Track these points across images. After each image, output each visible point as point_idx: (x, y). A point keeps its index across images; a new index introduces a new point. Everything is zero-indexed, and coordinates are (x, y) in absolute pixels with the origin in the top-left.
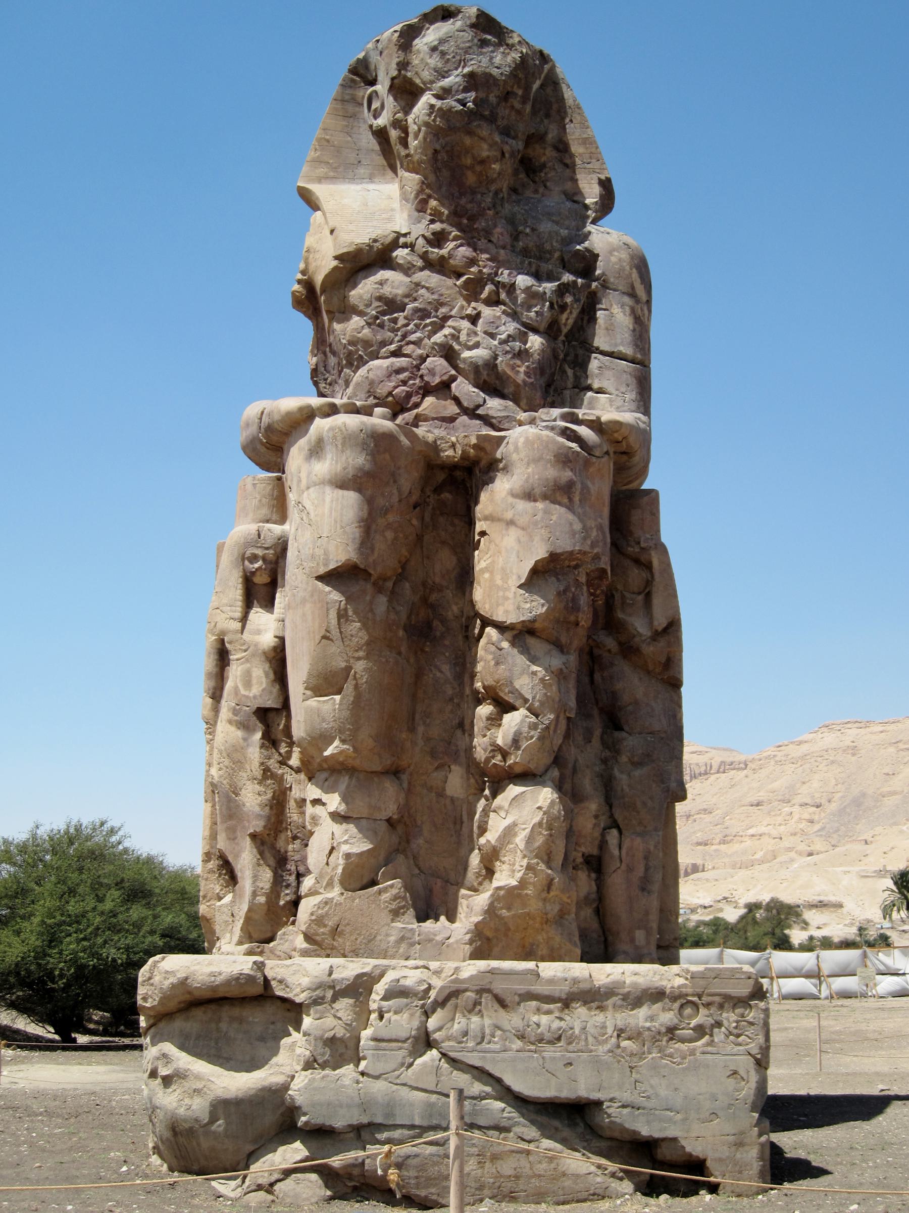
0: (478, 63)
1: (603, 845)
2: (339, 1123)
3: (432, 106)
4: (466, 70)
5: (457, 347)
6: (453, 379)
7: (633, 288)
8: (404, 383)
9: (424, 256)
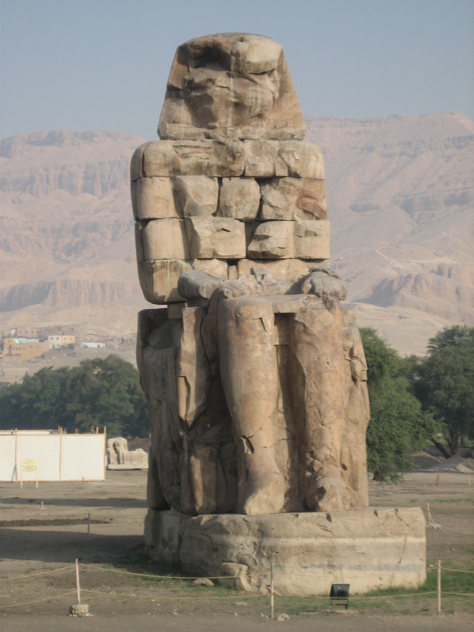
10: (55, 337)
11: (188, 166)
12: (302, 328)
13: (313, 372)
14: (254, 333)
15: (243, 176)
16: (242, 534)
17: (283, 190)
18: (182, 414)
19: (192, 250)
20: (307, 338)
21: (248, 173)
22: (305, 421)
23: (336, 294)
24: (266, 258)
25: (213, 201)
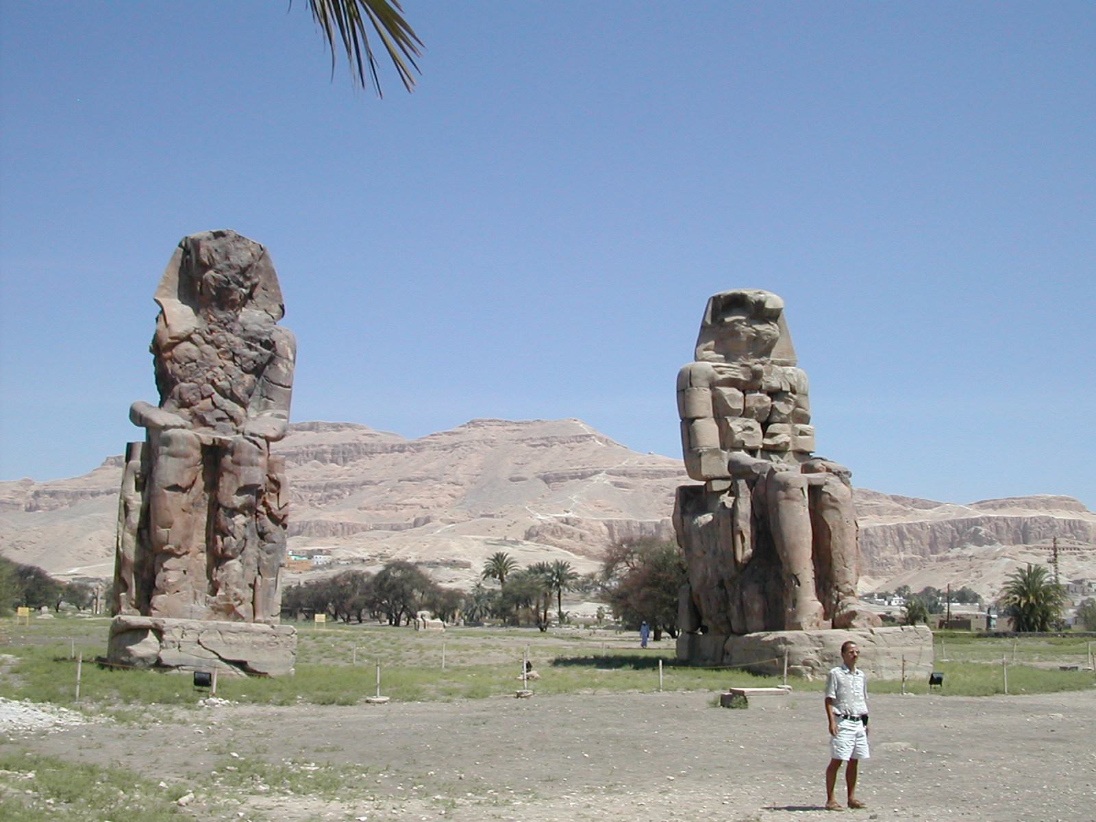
0: (234, 260)
1: (255, 581)
2: (173, 665)
3: (214, 277)
4: (228, 262)
5: (216, 380)
6: (213, 393)
7: (287, 355)
8: (194, 394)
9: (204, 339)
10: (318, 556)
11: (724, 379)
12: (828, 496)
13: (837, 529)
14: (799, 499)
15: (760, 390)
16: (807, 645)
17: (787, 402)
18: (740, 558)
19: (727, 439)
20: (833, 504)
21: (764, 387)
22: (830, 564)
23: (847, 473)
24: (778, 450)
25: (740, 406)
